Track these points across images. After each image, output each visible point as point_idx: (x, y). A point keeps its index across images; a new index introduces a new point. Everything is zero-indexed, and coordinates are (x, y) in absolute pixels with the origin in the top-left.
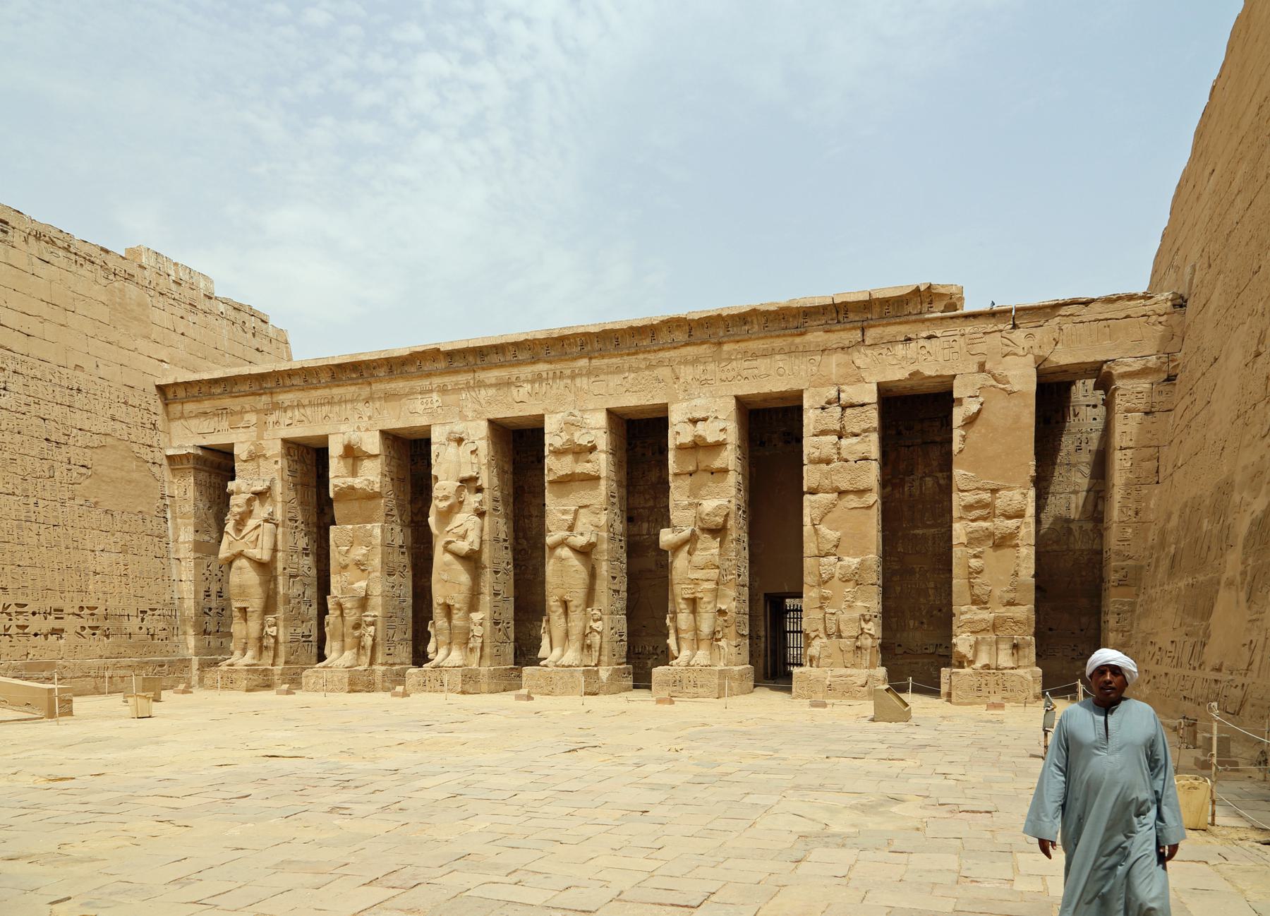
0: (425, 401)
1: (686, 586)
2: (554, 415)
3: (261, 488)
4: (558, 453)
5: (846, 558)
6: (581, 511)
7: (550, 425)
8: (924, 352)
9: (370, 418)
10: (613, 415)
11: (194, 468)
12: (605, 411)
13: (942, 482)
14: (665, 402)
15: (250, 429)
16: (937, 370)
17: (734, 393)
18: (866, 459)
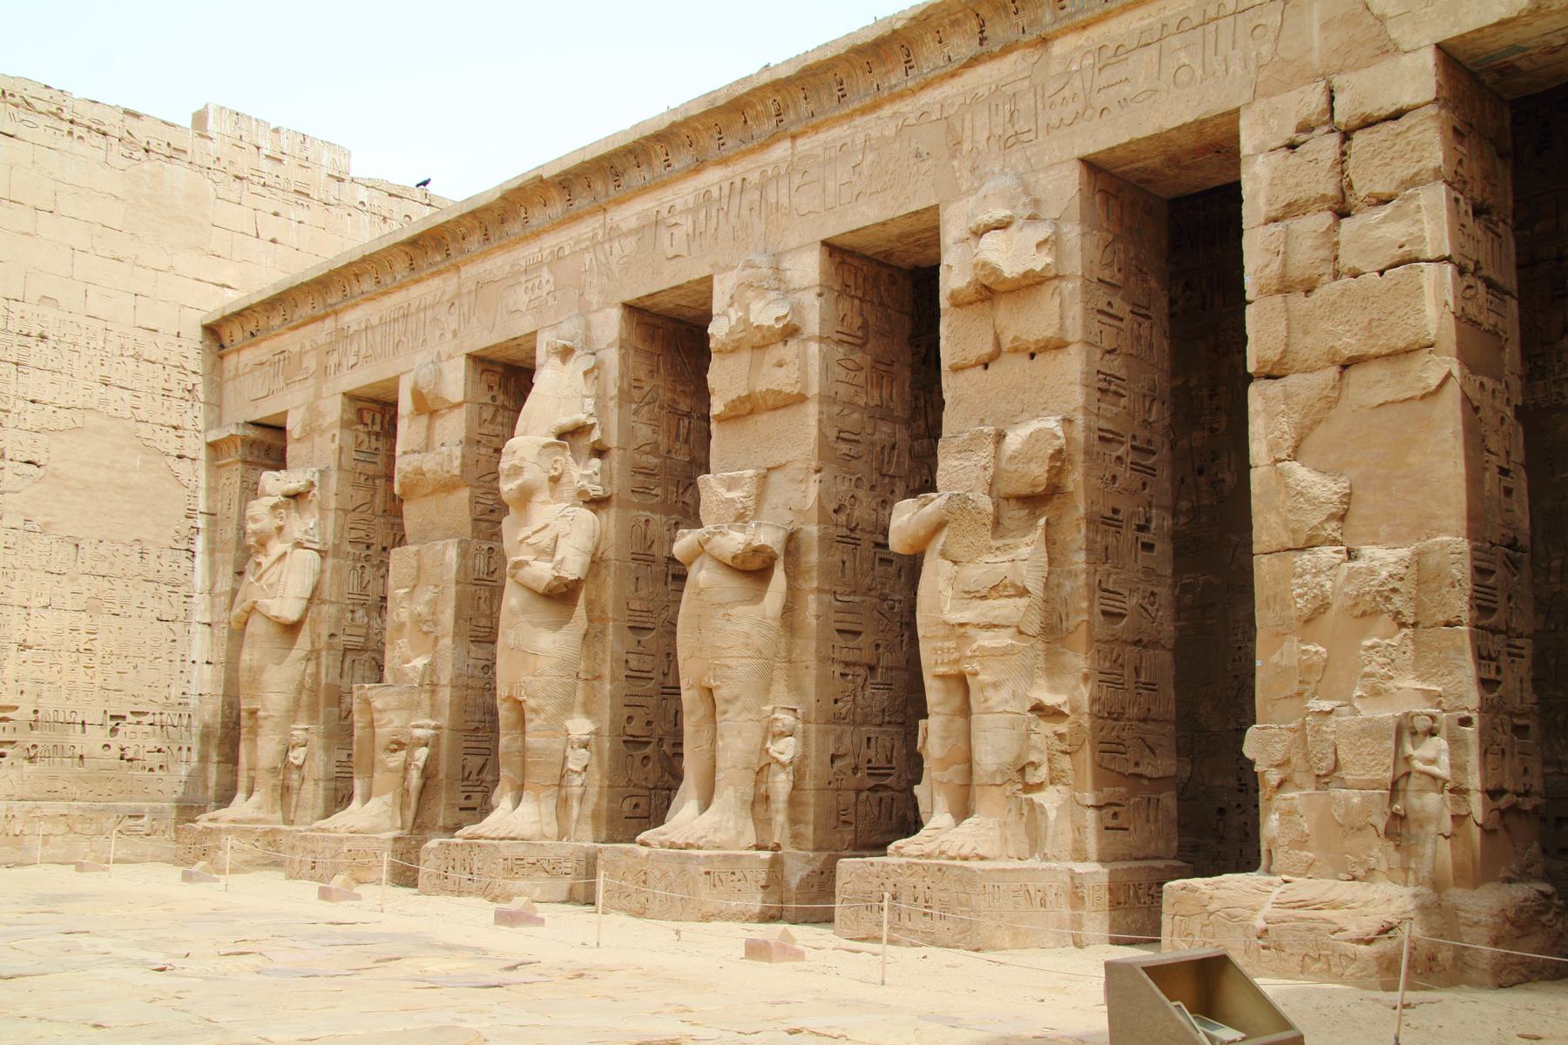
5: (1367, 550)
9: (455, 334)
10: (837, 251)
11: (245, 462)
12: (818, 245)
14: (933, 202)
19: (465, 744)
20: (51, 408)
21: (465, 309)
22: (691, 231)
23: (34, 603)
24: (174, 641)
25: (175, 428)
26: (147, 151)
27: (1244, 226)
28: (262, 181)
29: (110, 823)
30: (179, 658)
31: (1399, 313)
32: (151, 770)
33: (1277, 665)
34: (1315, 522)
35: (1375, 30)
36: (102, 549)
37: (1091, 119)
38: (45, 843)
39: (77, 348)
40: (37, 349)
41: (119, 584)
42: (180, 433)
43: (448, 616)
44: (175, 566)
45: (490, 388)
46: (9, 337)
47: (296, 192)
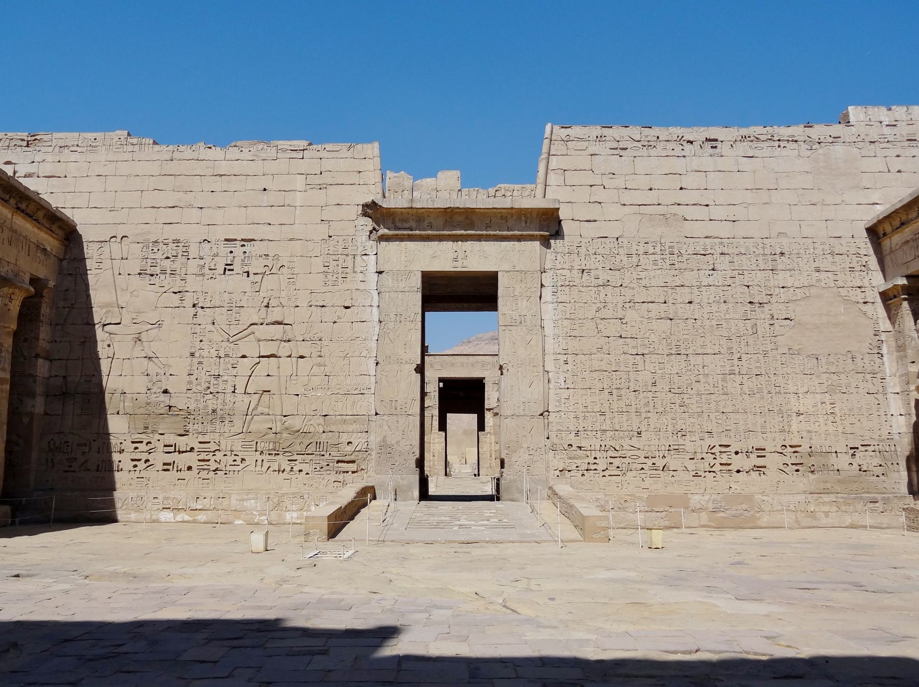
20: (792, 289)
23: (800, 391)
24: (879, 404)
25: (859, 287)
26: (819, 143)
28: (886, 140)
29: (860, 506)
30: (883, 414)
32: (878, 476)
36: (831, 359)
38: (827, 516)
39: (800, 256)
40: (781, 260)
41: (843, 376)
42: (863, 290)
44: (872, 363)
46: (766, 257)
47: (908, 140)
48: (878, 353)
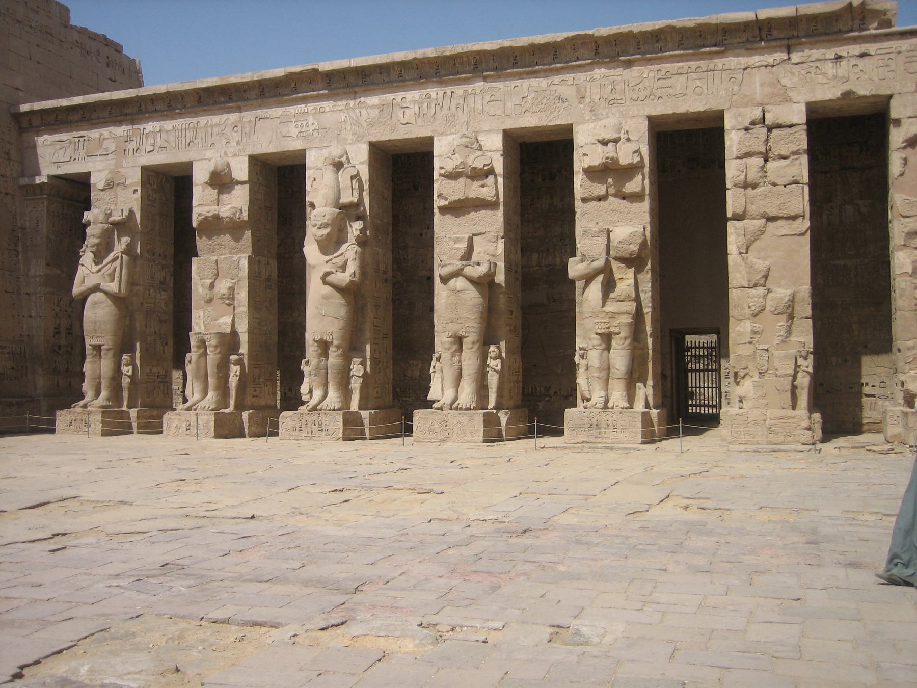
0: (299, 124)
1: (600, 320)
2: (444, 137)
3: (120, 218)
4: (452, 176)
5: (778, 290)
6: (475, 238)
7: (439, 148)
8: (857, 70)
9: (238, 143)
10: (508, 135)
13: (863, 210)
14: (570, 122)
15: (109, 157)
16: (872, 90)
17: (647, 113)
18: (796, 183)
19: (253, 363)
21: (247, 130)
22: (417, 112)
27: (726, 158)
31: (792, 202)
33: (739, 331)
34: (757, 278)
35: (782, 91)
37: (653, 100)
42: (5, 179)
43: (242, 296)
45: (257, 174)
48: (14, 250)
